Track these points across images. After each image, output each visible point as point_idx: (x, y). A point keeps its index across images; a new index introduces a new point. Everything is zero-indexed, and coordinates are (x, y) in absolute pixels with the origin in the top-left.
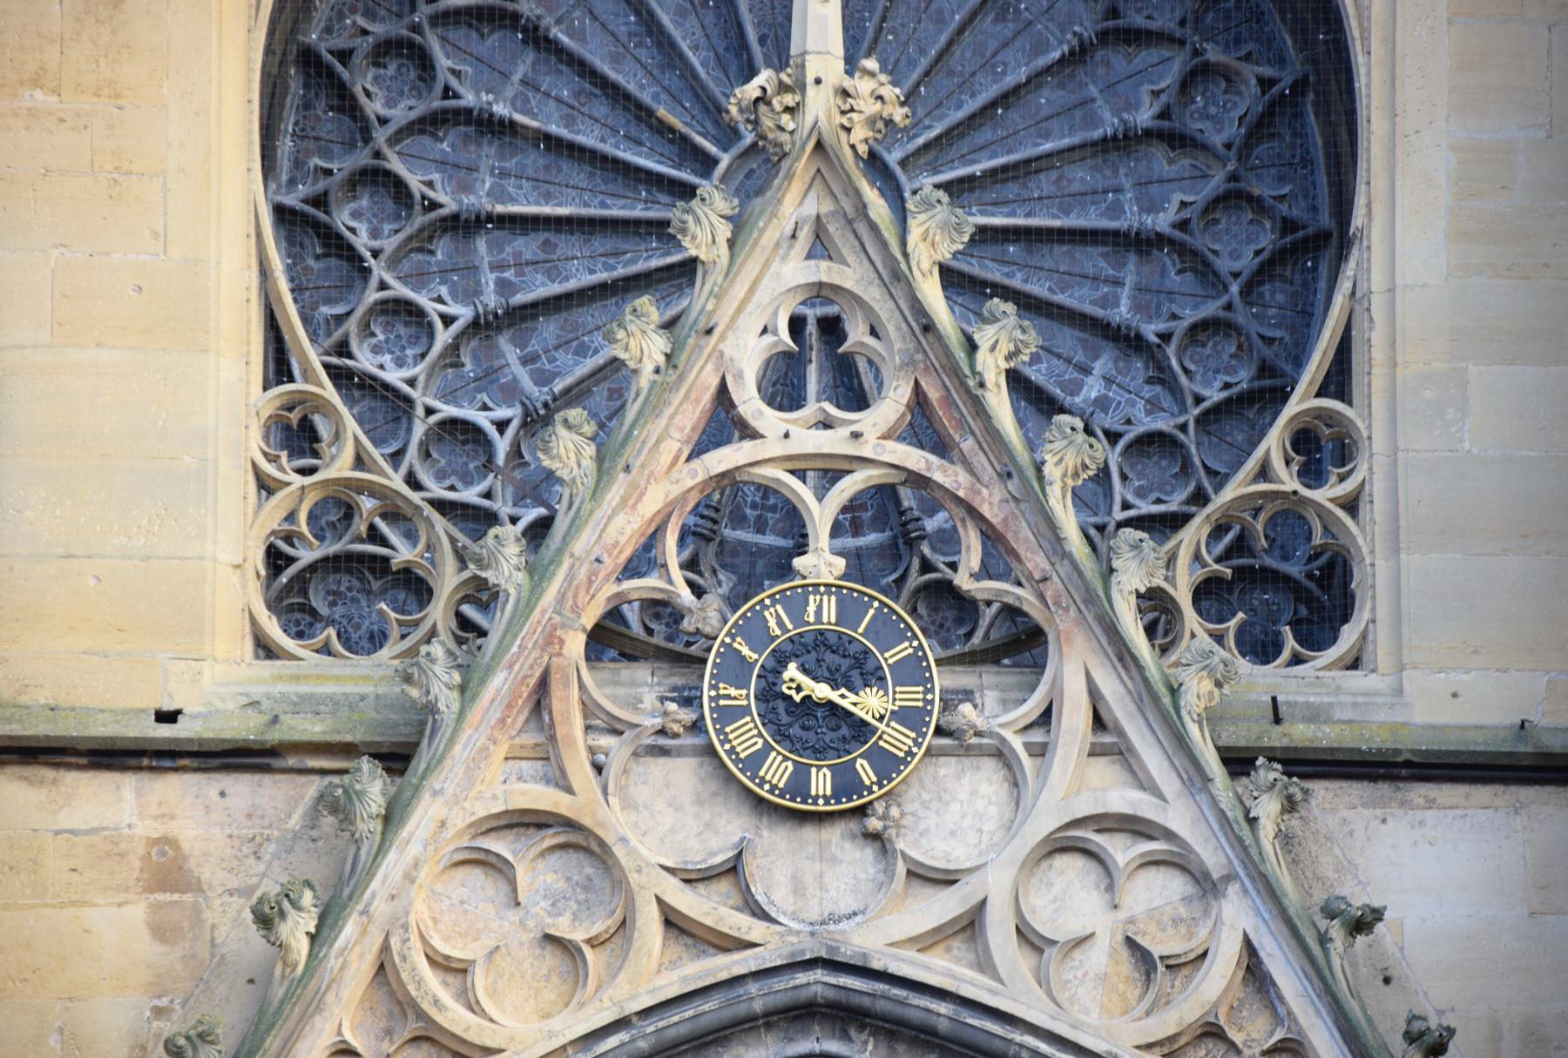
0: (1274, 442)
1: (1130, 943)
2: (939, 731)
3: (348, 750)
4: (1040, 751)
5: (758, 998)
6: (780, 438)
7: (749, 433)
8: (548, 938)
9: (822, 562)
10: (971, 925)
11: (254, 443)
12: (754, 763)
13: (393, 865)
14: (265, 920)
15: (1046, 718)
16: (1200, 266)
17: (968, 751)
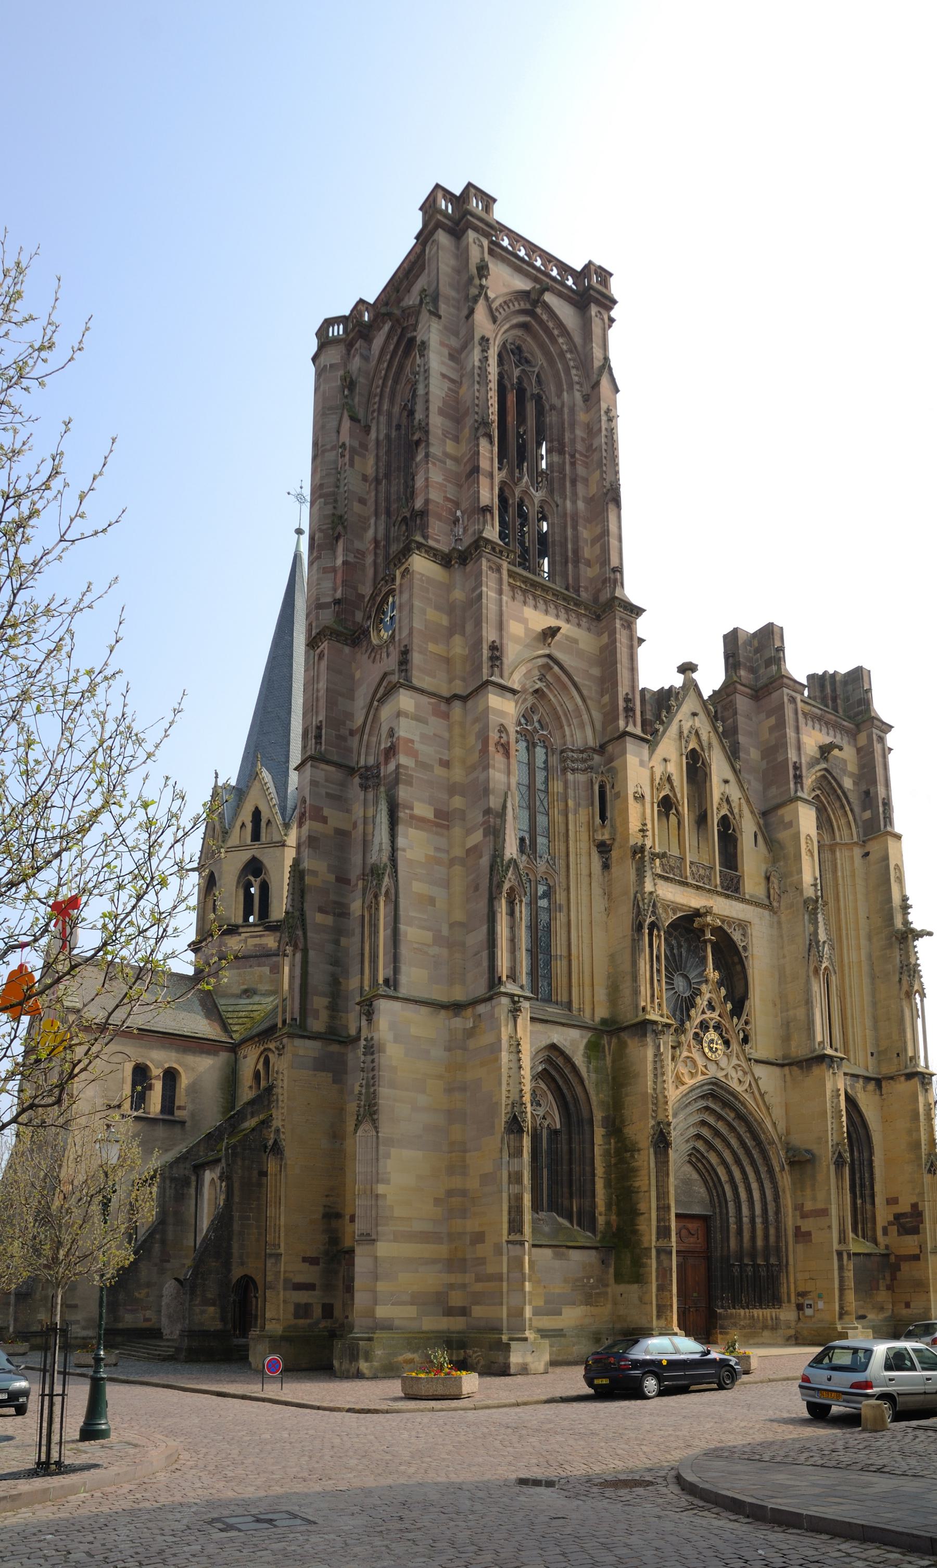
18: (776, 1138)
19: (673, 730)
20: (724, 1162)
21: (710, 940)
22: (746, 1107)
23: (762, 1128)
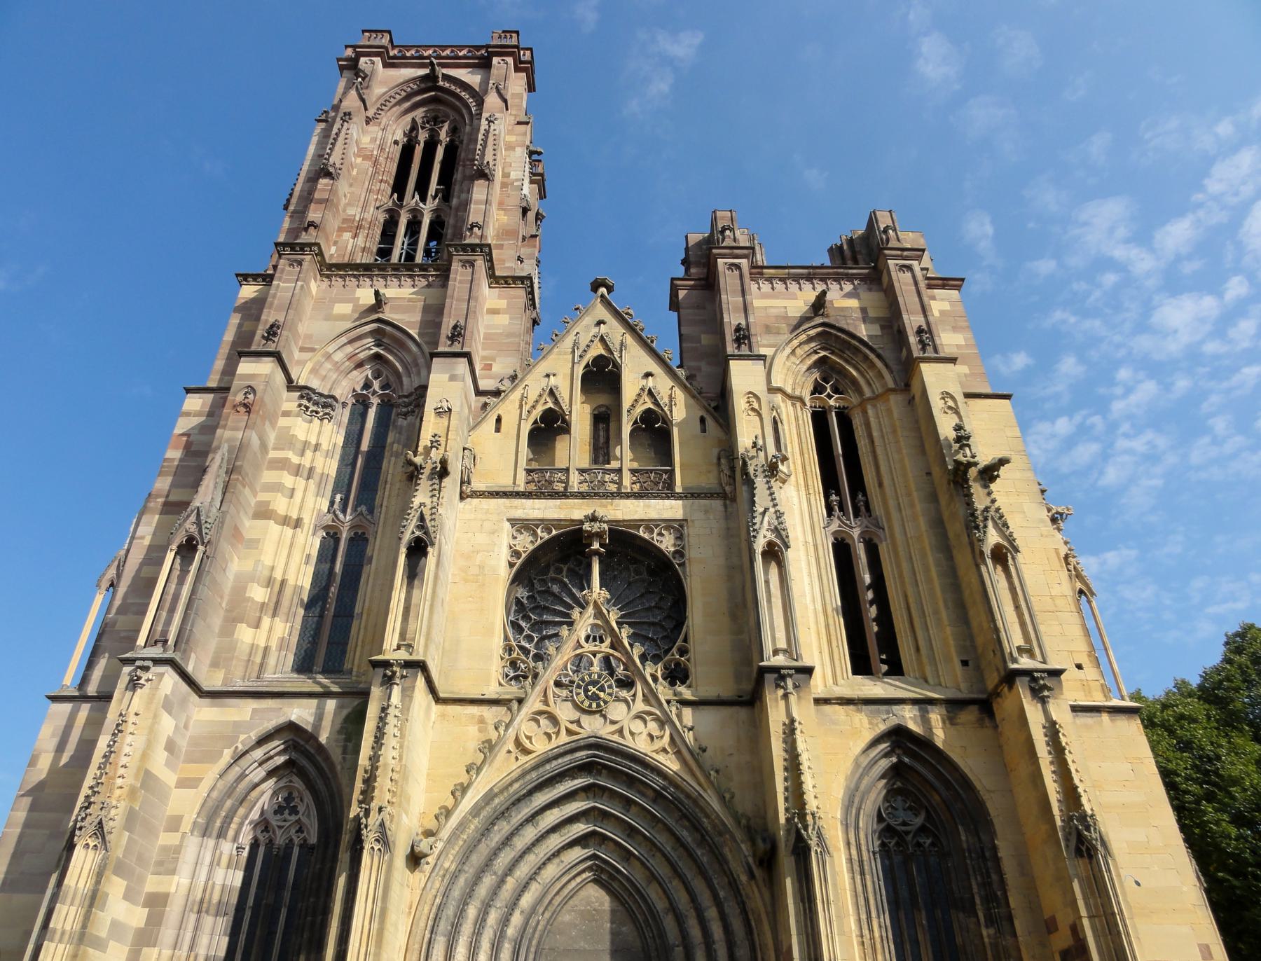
0: (674, 650)
3: (510, 700)
4: (634, 701)
5: (582, 743)
6: (589, 647)
11: (501, 652)
14: (496, 728)
15: (634, 695)
16: (662, 627)
18: (729, 822)
19: (568, 342)
21: (596, 553)
23: (702, 810)
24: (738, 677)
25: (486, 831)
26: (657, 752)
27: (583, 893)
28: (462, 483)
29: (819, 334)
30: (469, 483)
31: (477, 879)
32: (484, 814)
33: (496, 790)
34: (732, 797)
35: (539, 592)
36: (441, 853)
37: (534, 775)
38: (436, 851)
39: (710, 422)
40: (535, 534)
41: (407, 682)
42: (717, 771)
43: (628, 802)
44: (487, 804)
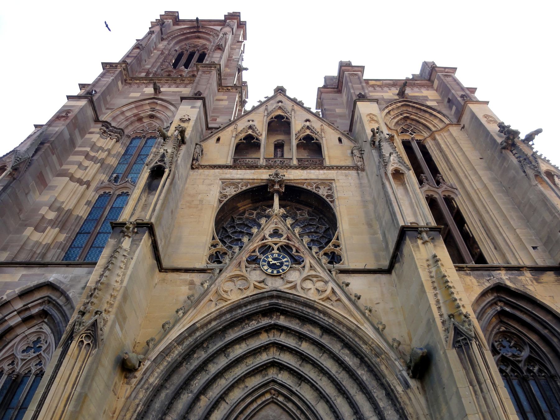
0: (330, 244)
1: (316, 289)
2: (290, 267)
5: (266, 295)
7: (266, 239)
8: (239, 289)
9: (275, 251)
10: (294, 287)
11: (210, 246)
12: (267, 270)
13: (219, 279)
15: (304, 267)
17: (294, 270)
18: (383, 345)
20: (322, 396)
22: (330, 316)
23: (360, 338)
24: (377, 258)
25: (187, 356)
26: (322, 300)
27: (263, 413)
28: (193, 159)
29: (402, 105)
30: (197, 160)
31: (177, 395)
32: (187, 343)
33: (198, 325)
34: (384, 328)
35: (237, 224)
36: (147, 369)
37: (228, 316)
38: (143, 368)
39: (344, 140)
40: (237, 187)
41: (137, 237)
42: (370, 311)
43: (302, 337)
44: (190, 335)
